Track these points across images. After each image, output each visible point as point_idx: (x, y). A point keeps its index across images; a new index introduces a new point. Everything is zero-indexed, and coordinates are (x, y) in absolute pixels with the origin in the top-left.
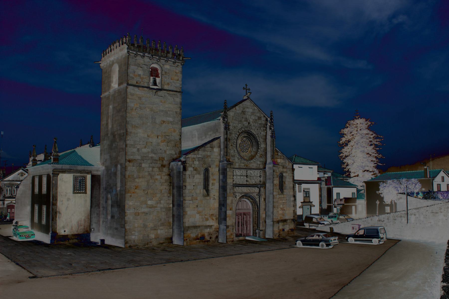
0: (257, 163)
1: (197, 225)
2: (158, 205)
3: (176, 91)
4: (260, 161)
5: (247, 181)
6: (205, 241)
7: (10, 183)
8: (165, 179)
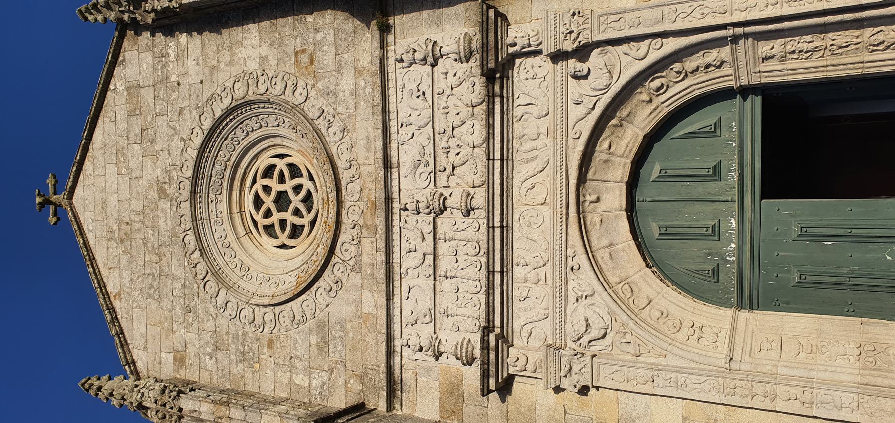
0: (351, 102)
4: (339, 71)
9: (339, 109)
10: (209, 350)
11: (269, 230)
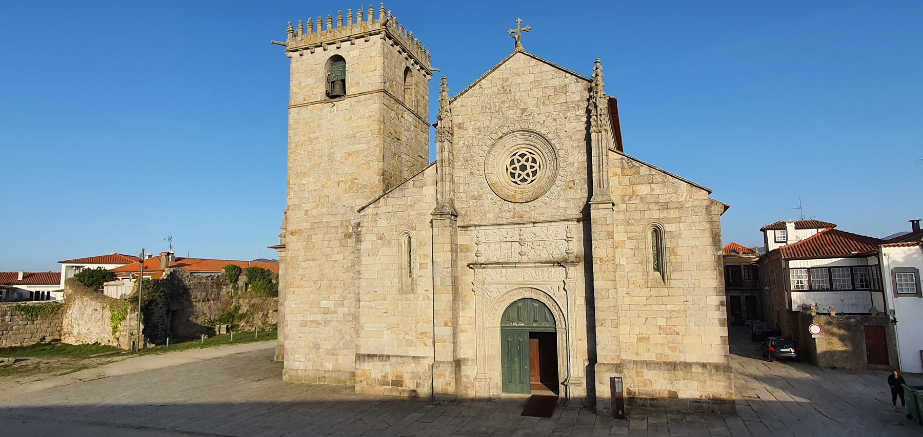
3: (372, 92)
4: (567, 200)
9: (553, 201)
10: (466, 143)
11: (512, 163)
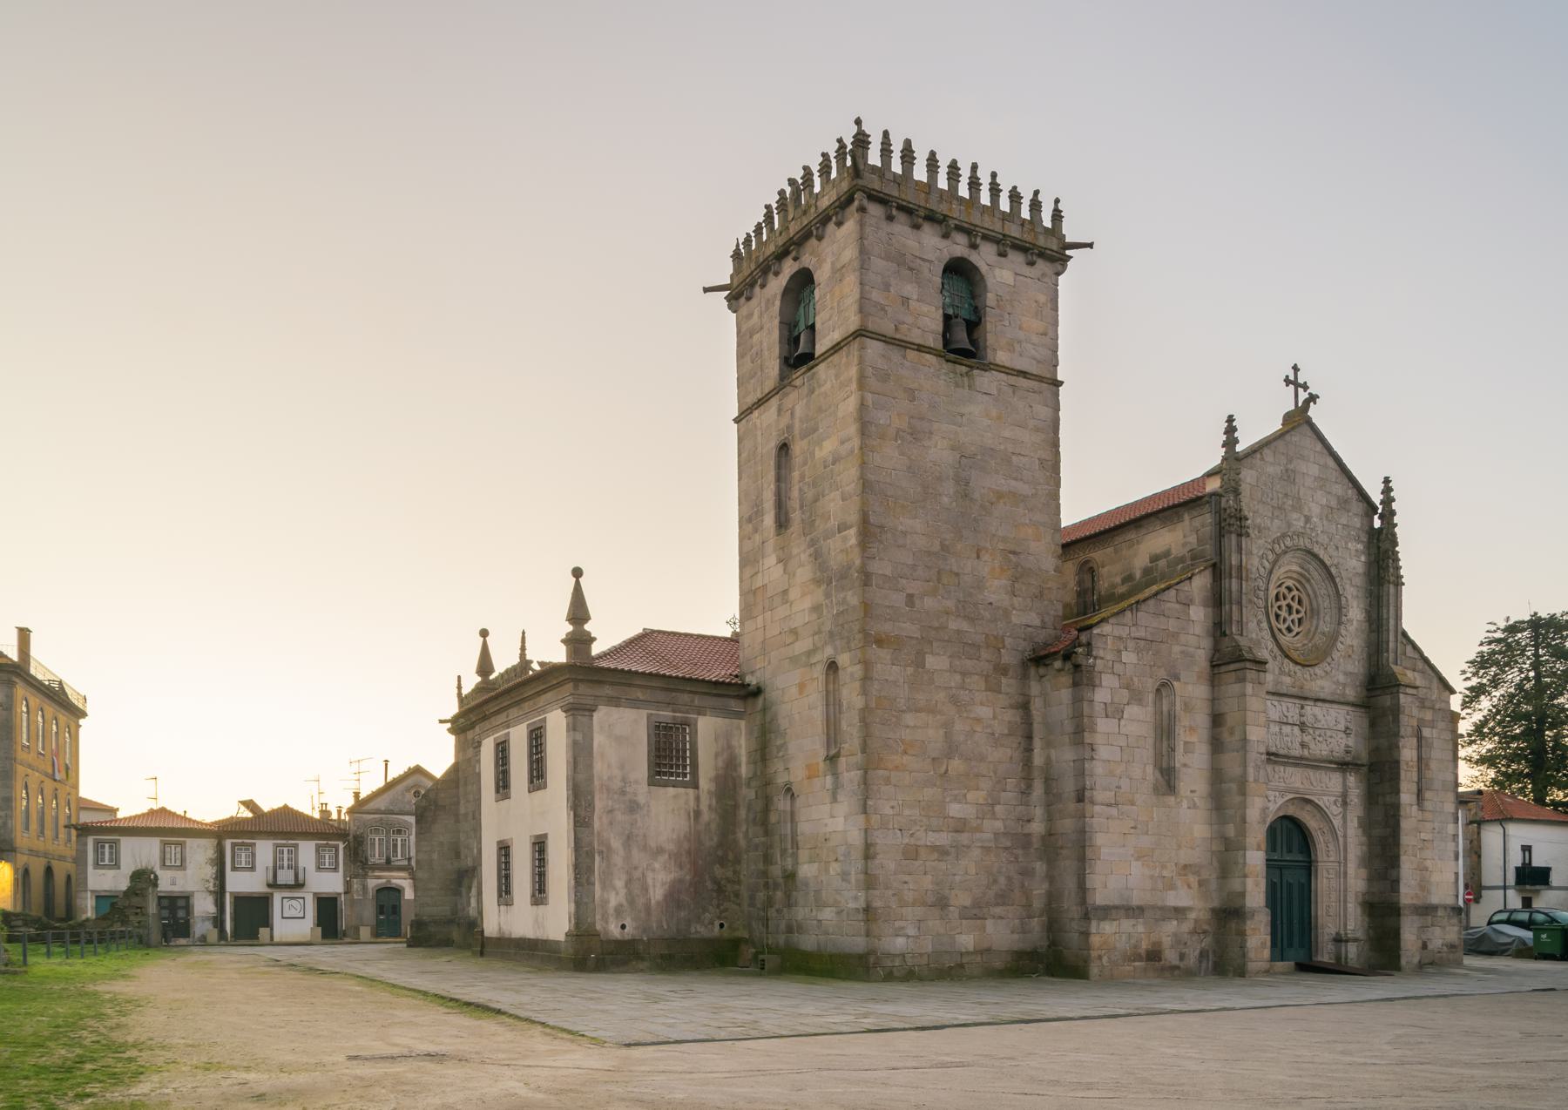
0: (1335, 679)
1: (1135, 902)
2: (987, 824)
5: (1303, 745)
6: (1163, 969)
7: (381, 819)
8: (1009, 722)
